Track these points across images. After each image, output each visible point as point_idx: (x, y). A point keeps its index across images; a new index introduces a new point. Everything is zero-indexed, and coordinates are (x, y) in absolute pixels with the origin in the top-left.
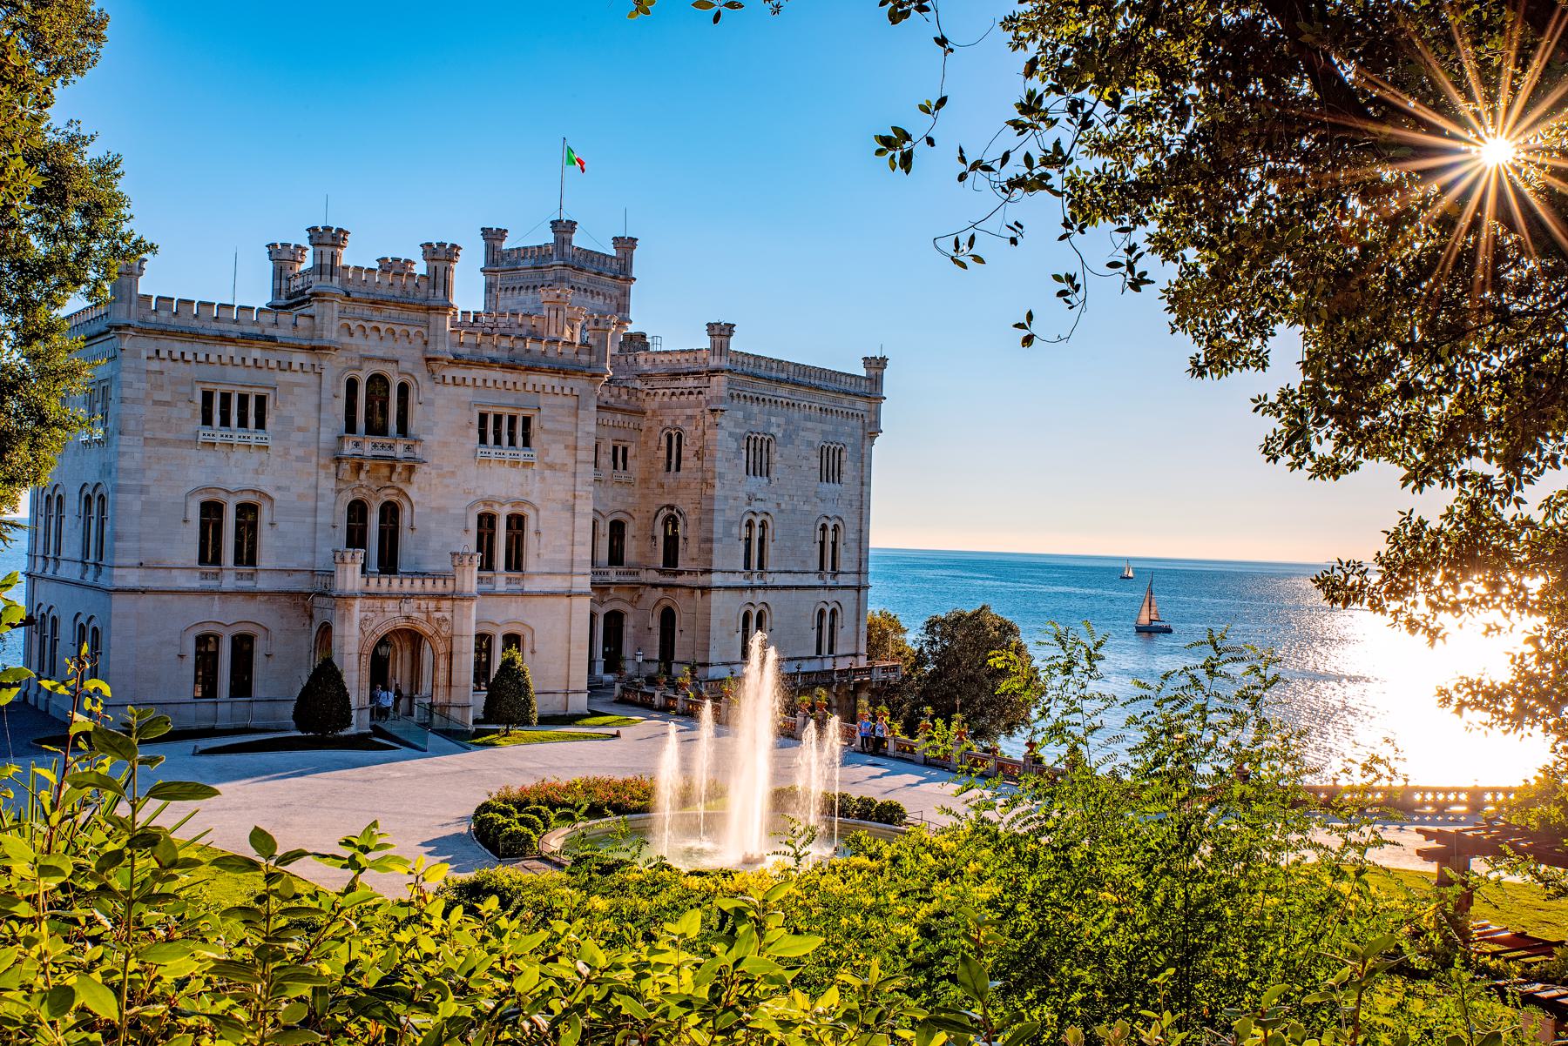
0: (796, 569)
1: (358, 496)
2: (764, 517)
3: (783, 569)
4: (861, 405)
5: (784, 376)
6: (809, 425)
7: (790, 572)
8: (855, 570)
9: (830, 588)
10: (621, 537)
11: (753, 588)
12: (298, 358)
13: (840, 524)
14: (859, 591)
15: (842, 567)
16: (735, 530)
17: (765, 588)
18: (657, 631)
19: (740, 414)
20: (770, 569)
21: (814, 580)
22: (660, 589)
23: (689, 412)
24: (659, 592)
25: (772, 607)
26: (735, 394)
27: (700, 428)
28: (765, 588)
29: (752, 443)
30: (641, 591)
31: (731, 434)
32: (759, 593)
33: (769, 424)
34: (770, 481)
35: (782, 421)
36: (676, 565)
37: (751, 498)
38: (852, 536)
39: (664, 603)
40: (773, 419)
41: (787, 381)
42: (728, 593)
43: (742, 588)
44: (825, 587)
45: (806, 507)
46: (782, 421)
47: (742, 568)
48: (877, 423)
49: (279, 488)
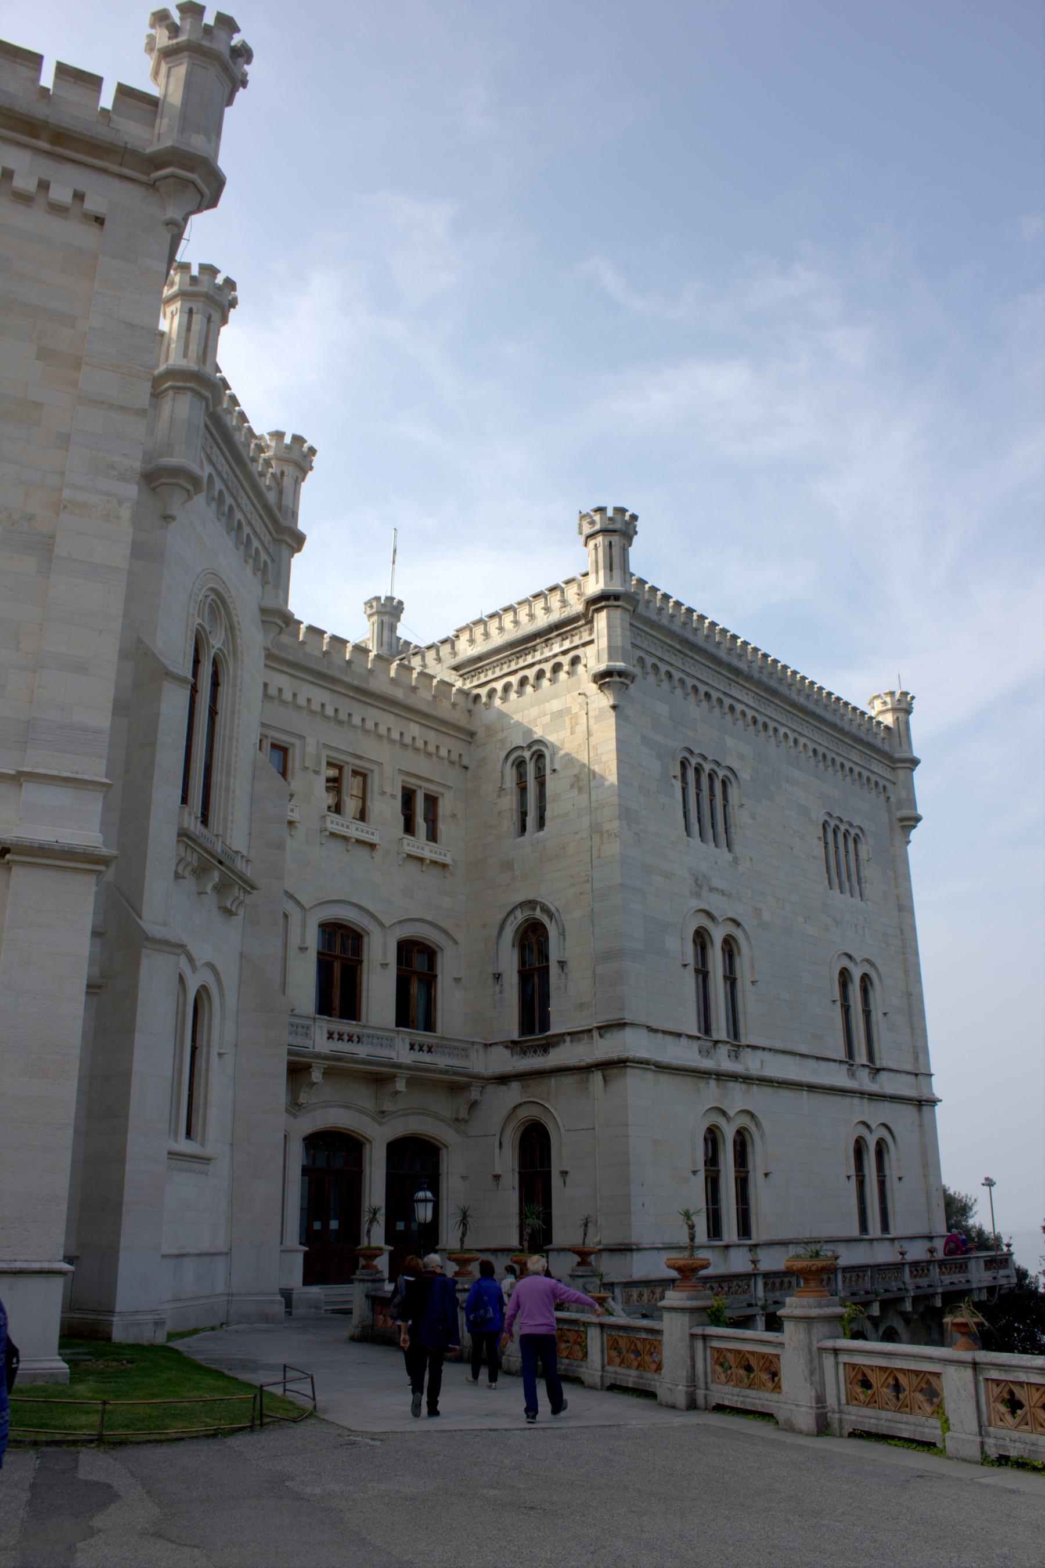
2: (731, 929)
3: (778, 1045)
8: (908, 1067)
10: (429, 980)
11: (721, 1077)
14: (920, 1111)
17: (747, 1080)
18: (511, 1181)
20: (753, 1040)
22: (515, 1085)
23: (555, 705)
24: (513, 1094)
25: (765, 1123)
26: (649, 661)
27: (581, 728)
28: (747, 1080)
29: (691, 775)
30: (474, 1094)
32: (737, 1089)
34: (736, 860)
36: (545, 1026)
37: (700, 884)
39: (524, 1114)
40: (730, 742)
43: (703, 1074)
44: (862, 1094)
48: (911, 801)
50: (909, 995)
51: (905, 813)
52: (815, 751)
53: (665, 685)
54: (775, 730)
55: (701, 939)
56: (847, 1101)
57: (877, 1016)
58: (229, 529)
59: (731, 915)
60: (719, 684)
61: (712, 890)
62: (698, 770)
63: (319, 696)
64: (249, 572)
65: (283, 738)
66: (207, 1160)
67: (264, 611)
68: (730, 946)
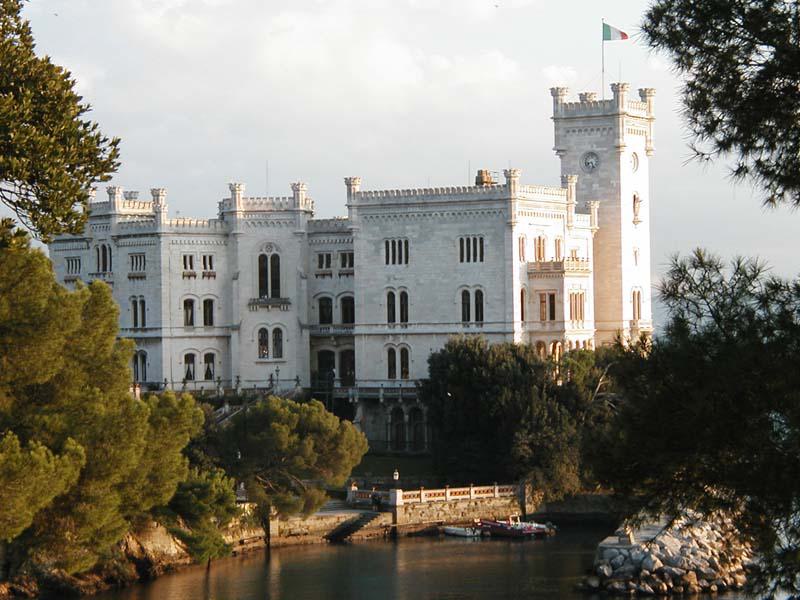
2: (403, 290)
3: (421, 321)
4: (497, 206)
6: (444, 226)
7: (429, 324)
11: (395, 335)
12: (85, 244)
13: (482, 290)
28: (407, 334)
31: (369, 241)
33: (404, 231)
35: (417, 227)
40: (407, 227)
45: (445, 281)
46: (417, 227)
47: (386, 322)
50: (504, 293)
53: (377, 221)
54: (430, 215)
55: (391, 296)
58: (268, 226)
61: (395, 279)
63: (333, 238)
64: (285, 228)
66: (284, 362)
67: (295, 233)
68: (404, 296)
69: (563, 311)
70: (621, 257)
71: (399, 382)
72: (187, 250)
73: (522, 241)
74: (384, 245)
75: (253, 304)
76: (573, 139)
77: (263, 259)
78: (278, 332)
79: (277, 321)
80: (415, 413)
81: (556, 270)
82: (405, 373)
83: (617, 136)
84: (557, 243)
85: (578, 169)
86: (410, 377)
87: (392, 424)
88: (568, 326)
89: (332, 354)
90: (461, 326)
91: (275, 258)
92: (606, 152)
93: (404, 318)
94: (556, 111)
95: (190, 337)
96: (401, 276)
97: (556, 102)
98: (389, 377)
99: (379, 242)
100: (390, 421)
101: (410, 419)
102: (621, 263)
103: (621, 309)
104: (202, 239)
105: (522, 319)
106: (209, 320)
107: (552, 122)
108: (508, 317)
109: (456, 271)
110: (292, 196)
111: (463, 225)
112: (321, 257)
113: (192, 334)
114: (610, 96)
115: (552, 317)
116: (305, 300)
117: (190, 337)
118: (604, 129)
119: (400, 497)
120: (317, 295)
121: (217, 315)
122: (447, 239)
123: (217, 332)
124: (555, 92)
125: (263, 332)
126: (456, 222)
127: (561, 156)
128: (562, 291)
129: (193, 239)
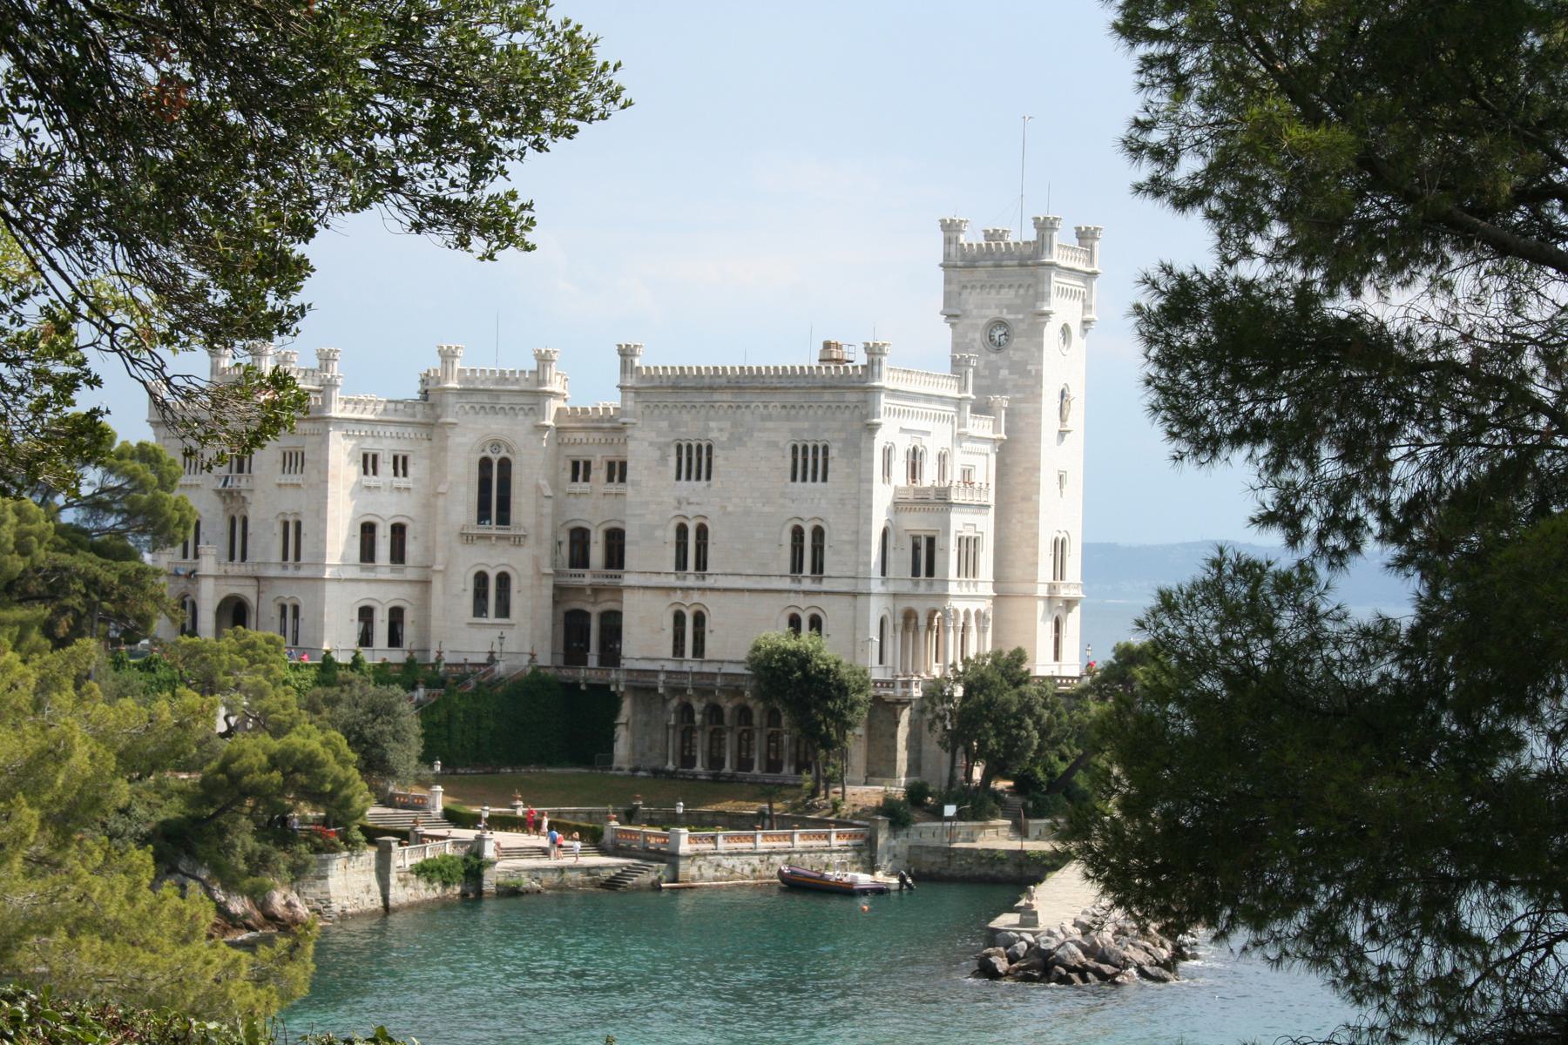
0: (750, 572)
1: (231, 512)
2: (701, 520)
4: (851, 397)
5: (723, 381)
6: (769, 425)
8: (853, 574)
9: (806, 593)
11: (681, 589)
15: (828, 570)
16: (658, 533)
17: (702, 590)
19: (664, 425)
21: (786, 584)
28: (702, 590)
31: (651, 444)
33: (707, 429)
34: (709, 486)
35: (727, 425)
38: (845, 537)
40: (712, 424)
41: (726, 388)
42: (648, 592)
44: (796, 592)
45: (767, 509)
46: (727, 425)
47: (673, 570)
49: (207, 511)
51: (869, 421)
52: (784, 407)
55: (682, 531)
56: (786, 595)
57: (826, 547)
59: (702, 513)
60: (699, 398)
61: (689, 504)
62: (689, 447)
63: (597, 436)
64: (520, 417)
65: (586, 458)
68: (702, 531)
69: (946, 564)
70: (1039, 484)
71: (690, 664)
72: (370, 445)
73: (887, 452)
74: (674, 451)
75: (467, 538)
76: (972, 299)
77: (485, 464)
78: (504, 579)
79: (504, 561)
80: (714, 712)
81: (941, 500)
82: (699, 650)
83: (1042, 296)
84: (942, 458)
85: (978, 344)
86: (707, 656)
87: (675, 727)
88: (953, 589)
89: (587, 615)
90: (788, 580)
91: (505, 465)
92: (1022, 321)
93: (701, 564)
94: (947, 256)
95: (368, 581)
96: (699, 501)
97: (948, 241)
98: (675, 654)
99: (668, 445)
100: (672, 722)
101: (703, 721)
102: (1038, 493)
103: (1036, 564)
104: (393, 429)
105: (883, 573)
106: (398, 555)
107: (941, 273)
108: (861, 569)
109: (783, 495)
110: (535, 368)
111: (795, 425)
112: (575, 465)
113: (371, 575)
114: (1031, 235)
115: (930, 572)
116: (547, 532)
117: (368, 581)
118: (1020, 286)
119: (685, 842)
120: (567, 522)
121: (412, 548)
122: (773, 445)
123: (410, 573)
124: (950, 229)
125: (481, 579)
126: (788, 420)
127: (953, 325)
128: (947, 533)
129: (379, 428)
